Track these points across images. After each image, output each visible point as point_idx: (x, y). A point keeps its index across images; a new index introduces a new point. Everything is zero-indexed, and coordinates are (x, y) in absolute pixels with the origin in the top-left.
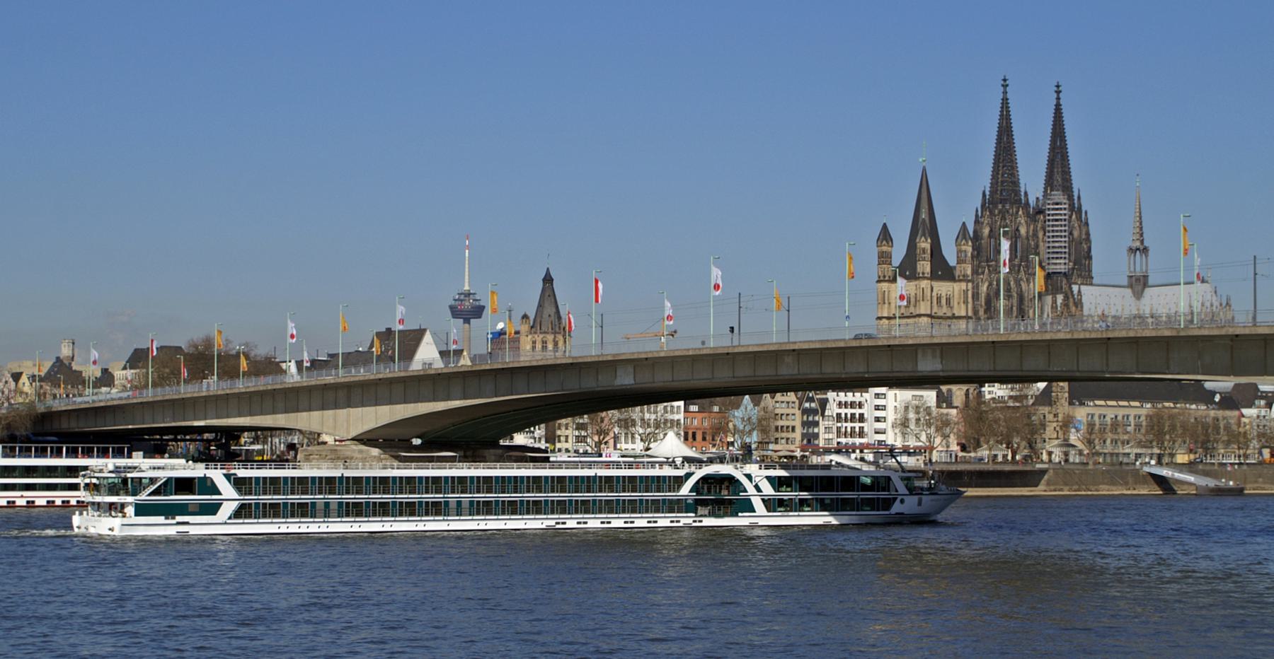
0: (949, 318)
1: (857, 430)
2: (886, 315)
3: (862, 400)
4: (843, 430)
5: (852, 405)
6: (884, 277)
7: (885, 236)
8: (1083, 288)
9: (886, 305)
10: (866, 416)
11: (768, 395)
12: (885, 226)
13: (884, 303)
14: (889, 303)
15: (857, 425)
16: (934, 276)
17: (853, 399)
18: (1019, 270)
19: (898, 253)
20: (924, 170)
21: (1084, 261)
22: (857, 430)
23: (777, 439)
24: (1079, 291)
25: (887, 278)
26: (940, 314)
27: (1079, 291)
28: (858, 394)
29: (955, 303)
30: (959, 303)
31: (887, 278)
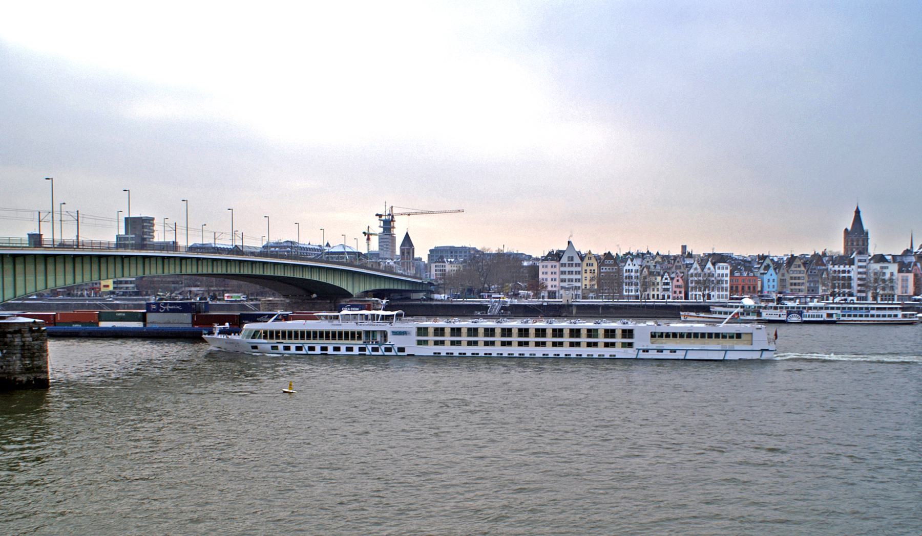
1: (846, 284)
3: (850, 269)
5: (844, 272)
10: (852, 278)
15: (846, 283)
17: (844, 269)
22: (846, 284)
23: (792, 290)
28: (847, 266)
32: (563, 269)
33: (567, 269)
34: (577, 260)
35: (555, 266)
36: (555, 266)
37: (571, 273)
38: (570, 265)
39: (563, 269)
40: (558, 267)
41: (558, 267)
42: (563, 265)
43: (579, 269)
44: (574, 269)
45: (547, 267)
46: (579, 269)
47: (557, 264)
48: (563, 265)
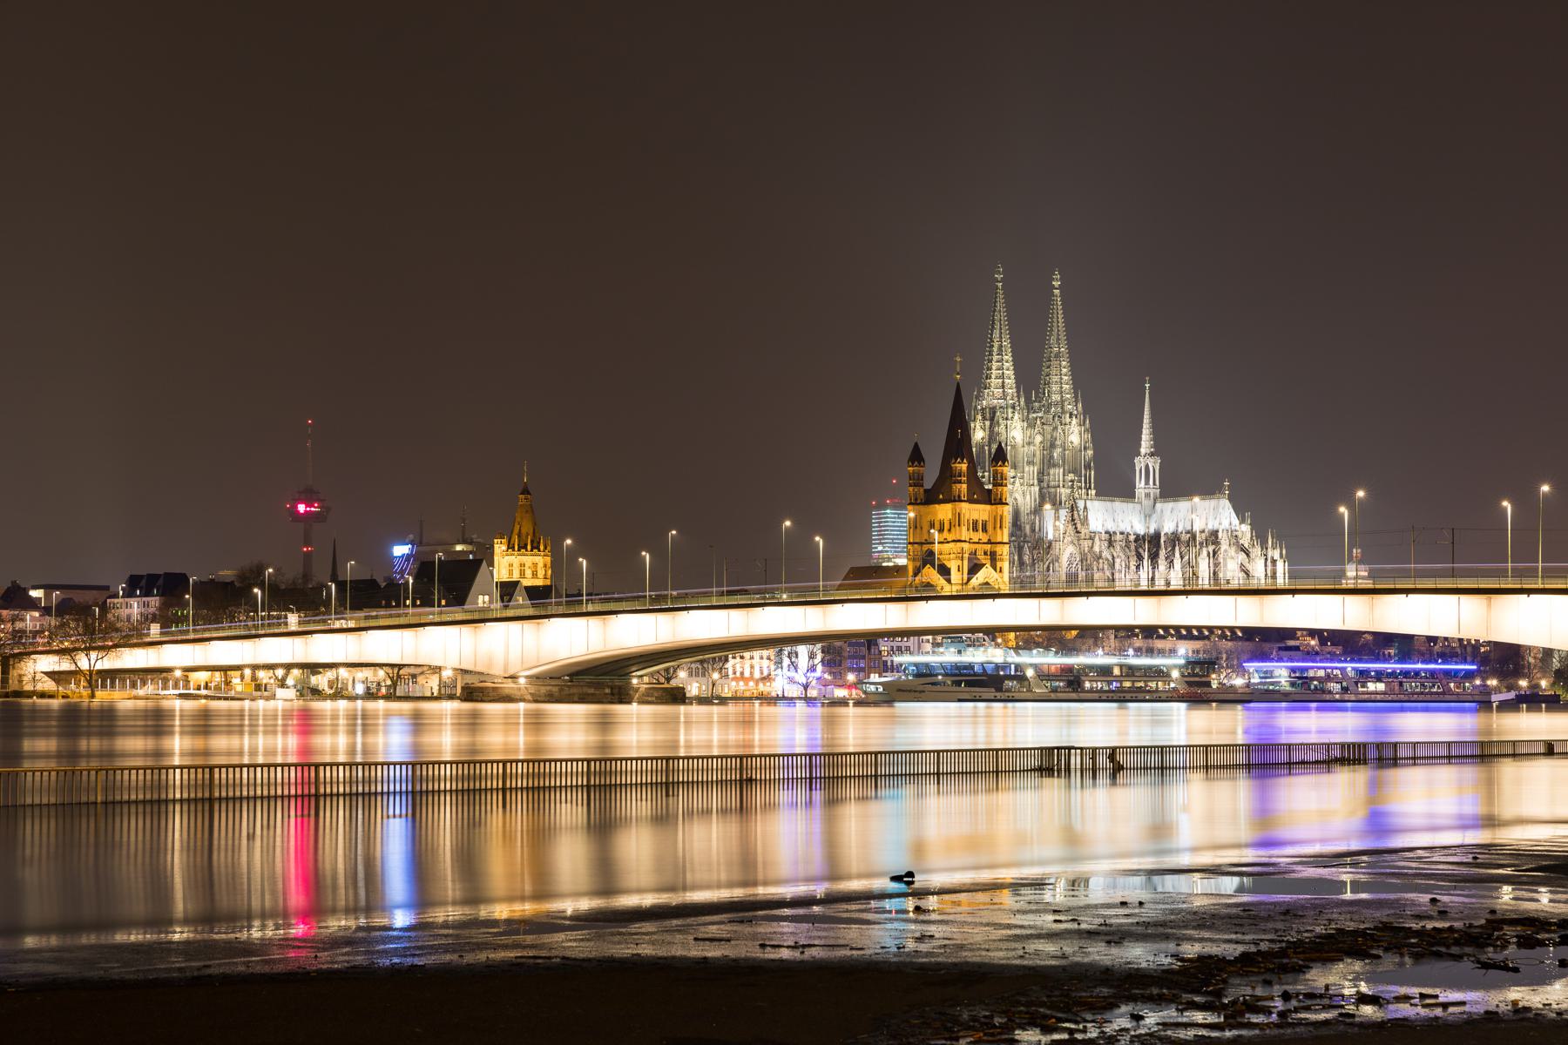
0: (984, 543)
4: (889, 664)
6: (916, 499)
7: (916, 457)
8: (1088, 503)
9: (918, 530)
11: (1525, 706)
12: (916, 446)
13: (916, 527)
14: (921, 528)
16: (971, 501)
19: (931, 475)
20: (958, 384)
24: (1085, 508)
25: (919, 501)
27: (1085, 508)
29: (990, 528)
30: (995, 528)
31: (919, 501)
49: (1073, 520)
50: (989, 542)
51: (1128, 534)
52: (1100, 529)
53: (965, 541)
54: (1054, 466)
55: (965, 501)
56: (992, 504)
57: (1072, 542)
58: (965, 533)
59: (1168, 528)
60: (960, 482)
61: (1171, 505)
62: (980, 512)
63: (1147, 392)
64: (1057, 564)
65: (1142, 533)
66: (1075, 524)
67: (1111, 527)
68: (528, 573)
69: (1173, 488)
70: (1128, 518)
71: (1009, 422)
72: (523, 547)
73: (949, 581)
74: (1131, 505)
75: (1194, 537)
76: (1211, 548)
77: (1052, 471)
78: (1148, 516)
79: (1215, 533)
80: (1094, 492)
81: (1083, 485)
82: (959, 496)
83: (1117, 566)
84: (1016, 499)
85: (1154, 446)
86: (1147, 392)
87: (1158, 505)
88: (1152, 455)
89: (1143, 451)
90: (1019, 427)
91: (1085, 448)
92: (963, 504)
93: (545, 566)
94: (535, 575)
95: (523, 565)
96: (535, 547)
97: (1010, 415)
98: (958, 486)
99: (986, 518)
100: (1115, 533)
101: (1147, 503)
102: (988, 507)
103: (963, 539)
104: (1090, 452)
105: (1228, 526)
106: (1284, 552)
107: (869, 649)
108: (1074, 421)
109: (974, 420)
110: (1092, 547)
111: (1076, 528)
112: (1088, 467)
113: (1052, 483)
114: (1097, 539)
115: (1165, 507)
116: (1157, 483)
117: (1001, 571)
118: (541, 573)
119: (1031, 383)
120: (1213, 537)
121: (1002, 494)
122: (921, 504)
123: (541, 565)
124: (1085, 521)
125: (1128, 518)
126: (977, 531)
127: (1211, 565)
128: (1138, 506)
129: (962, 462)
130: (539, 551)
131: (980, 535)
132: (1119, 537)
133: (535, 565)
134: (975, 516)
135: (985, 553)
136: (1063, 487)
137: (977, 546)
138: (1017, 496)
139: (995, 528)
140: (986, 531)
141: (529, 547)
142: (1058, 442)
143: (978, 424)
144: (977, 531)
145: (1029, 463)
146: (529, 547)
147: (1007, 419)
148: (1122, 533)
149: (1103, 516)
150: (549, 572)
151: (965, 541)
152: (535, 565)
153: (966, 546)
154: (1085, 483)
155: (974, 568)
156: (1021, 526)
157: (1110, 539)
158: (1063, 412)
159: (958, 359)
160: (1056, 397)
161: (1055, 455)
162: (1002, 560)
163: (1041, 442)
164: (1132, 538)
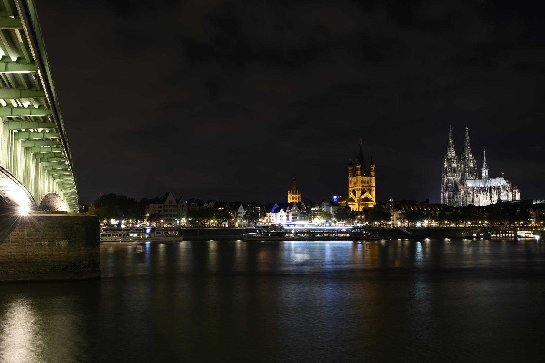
2: (351, 187)
9: (351, 184)
16: (362, 175)
18: (454, 177)
21: (474, 174)
24: (466, 181)
26: (365, 186)
29: (369, 183)
32: (166, 208)
33: (168, 208)
34: (174, 203)
35: (161, 207)
36: (161, 207)
37: (171, 211)
38: (171, 206)
39: (166, 208)
40: (162, 207)
41: (162, 207)
42: (166, 206)
43: (176, 209)
44: (173, 209)
45: (156, 207)
46: (176, 209)
47: (162, 205)
48: (166, 206)
49: (463, 184)
50: (369, 186)
51: (479, 187)
52: (470, 186)
53: (360, 186)
54: (466, 172)
55: (359, 176)
56: (369, 176)
57: (463, 190)
58: (360, 184)
59: (489, 186)
60: (358, 171)
61: (490, 180)
62: (366, 178)
63: (484, 152)
64: (460, 195)
65: (483, 187)
66: (464, 185)
67: (474, 186)
68: (294, 199)
69: (492, 175)
70: (480, 184)
71: (452, 162)
72: (293, 193)
73: (356, 197)
74: (480, 180)
75: (495, 188)
76: (497, 190)
77: (465, 174)
78: (485, 183)
79: (499, 186)
80: (477, 178)
81: (474, 176)
82: (358, 174)
83: (474, 195)
84: (455, 180)
85: (487, 166)
86: (484, 152)
87: (488, 180)
88: (486, 168)
89: (484, 167)
90: (455, 163)
91: (475, 168)
92: (359, 177)
93: (299, 197)
94: (296, 199)
95: (293, 197)
96: (296, 193)
97: (453, 160)
98: (357, 172)
99: (368, 180)
100: (475, 187)
101: (485, 180)
102: (369, 177)
103: (359, 185)
104: (476, 169)
105: (502, 184)
106: (519, 191)
107: (308, 214)
108: (471, 161)
109: (445, 162)
110: (468, 191)
111: (464, 186)
112: (476, 172)
113: (466, 176)
114: (469, 188)
115: (489, 180)
116: (488, 175)
117: (372, 194)
118: (297, 199)
119: (460, 154)
120: (499, 188)
121: (372, 174)
122: (352, 177)
123: (297, 197)
124: (466, 185)
125: (480, 184)
126: (365, 183)
127: (498, 194)
128: (482, 181)
129: (372, 166)
130: (297, 193)
131: (366, 184)
132: (476, 188)
133: (296, 197)
134: (365, 180)
135: (368, 189)
136: (469, 177)
137: (365, 187)
138: (455, 179)
139: (370, 183)
140: (368, 183)
141: (295, 193)
142: (467, 166)
143: (445, 163)
144: (365, 183)
145: (458, 172)
146: (295, 193)
147: (452, 161)
148: (476, 187)
149: (470, 184)
150: (300, 199)
151: (360, 186)
152: (296, 197)
153: (360, 187)
154: (475, 176)
155: (363, 192)
156: (456, 187)
157: (473, 189)
158: (469, 159)
159: (361, 139)
160: (467, 156)
161: (466, 169)
162: (372, 191)
163: (463, 167)
164: (480, 188)
